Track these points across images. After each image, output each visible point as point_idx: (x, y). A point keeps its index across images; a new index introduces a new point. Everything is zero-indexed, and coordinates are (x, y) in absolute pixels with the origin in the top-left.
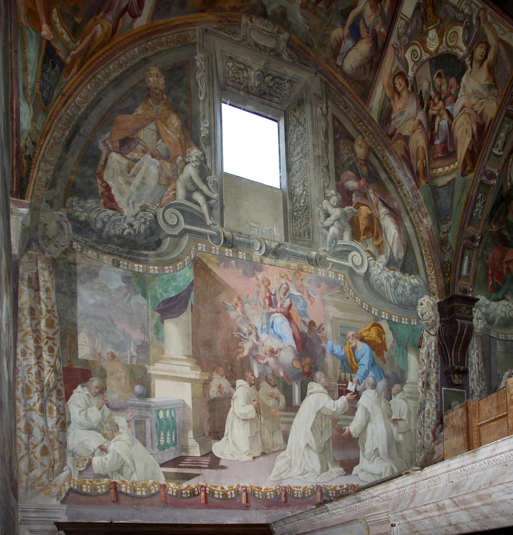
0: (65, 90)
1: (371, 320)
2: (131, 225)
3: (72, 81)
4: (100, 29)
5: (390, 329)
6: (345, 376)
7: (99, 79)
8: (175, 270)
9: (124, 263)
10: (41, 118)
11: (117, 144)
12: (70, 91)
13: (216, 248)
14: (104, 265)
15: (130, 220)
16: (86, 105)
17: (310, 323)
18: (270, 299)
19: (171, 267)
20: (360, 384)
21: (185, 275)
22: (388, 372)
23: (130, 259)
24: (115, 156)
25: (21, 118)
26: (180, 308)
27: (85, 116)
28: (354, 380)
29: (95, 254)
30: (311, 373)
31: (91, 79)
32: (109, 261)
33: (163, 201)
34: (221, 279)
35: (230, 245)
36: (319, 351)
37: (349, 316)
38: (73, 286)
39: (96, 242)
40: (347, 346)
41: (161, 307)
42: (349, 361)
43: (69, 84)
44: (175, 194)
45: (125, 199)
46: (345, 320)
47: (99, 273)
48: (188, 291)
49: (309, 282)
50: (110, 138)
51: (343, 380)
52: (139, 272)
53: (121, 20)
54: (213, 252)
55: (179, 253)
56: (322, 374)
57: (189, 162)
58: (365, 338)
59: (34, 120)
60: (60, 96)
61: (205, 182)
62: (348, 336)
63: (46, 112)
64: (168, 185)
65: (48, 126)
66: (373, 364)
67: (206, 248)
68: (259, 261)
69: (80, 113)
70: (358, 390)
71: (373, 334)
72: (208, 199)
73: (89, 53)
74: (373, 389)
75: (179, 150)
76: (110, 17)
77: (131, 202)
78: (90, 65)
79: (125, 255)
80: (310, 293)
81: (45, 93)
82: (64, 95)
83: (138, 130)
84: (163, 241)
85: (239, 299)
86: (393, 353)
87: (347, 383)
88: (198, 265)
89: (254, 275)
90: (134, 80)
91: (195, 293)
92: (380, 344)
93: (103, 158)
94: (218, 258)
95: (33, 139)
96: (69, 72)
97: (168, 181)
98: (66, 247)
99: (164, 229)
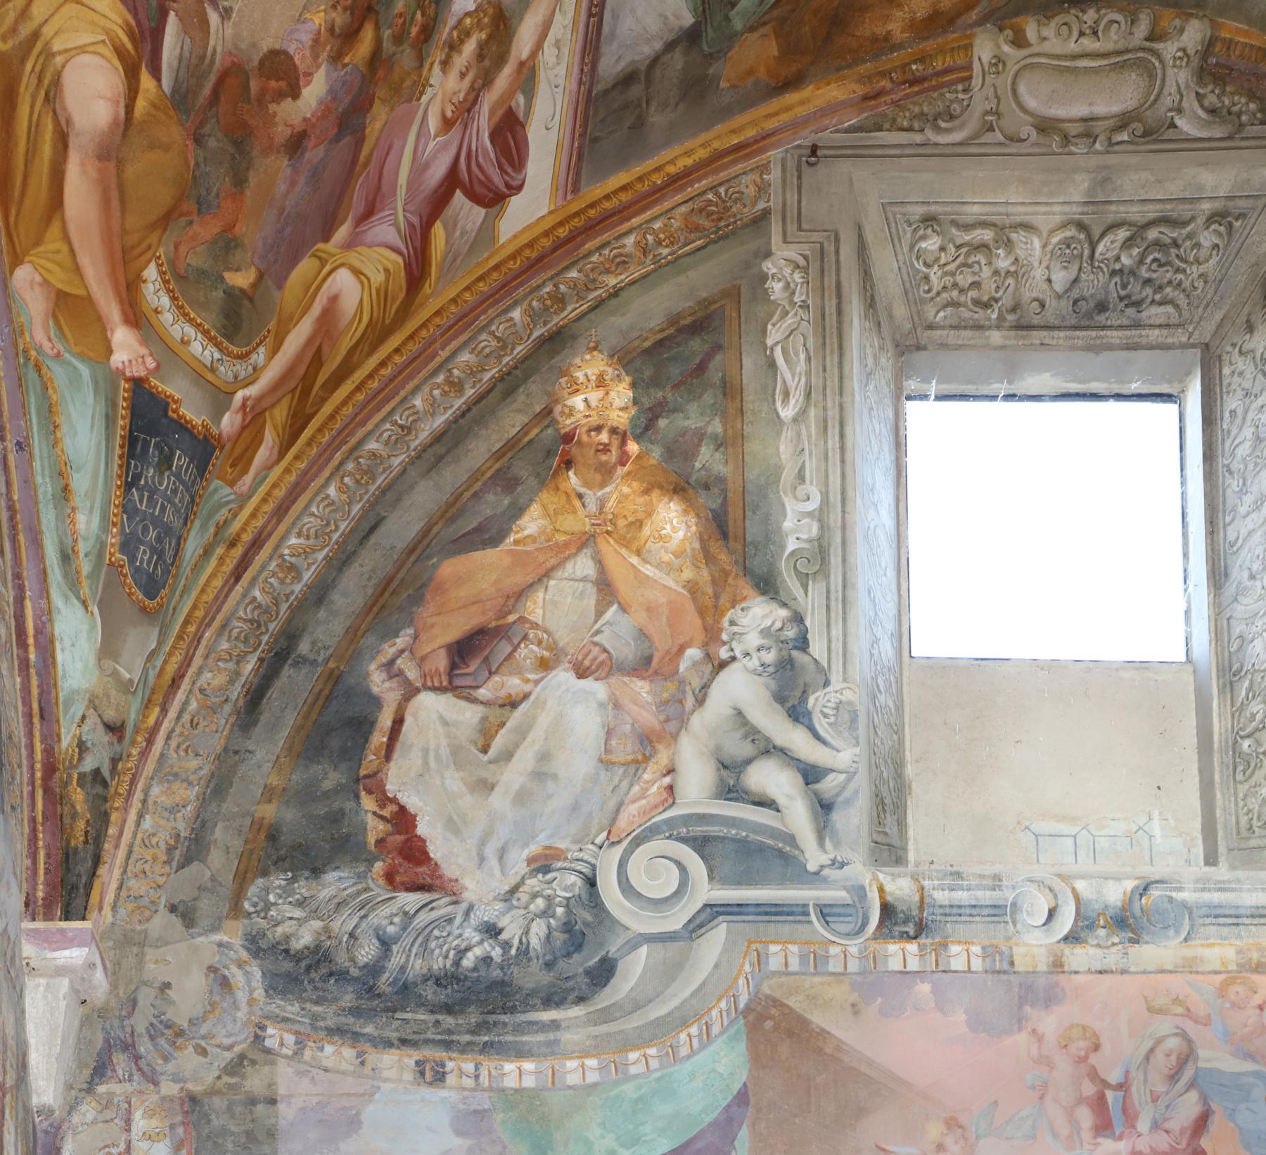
2: (492, 931)
4: (351, 278)
8: (672, 1056)
9: (460, 1067)
10: (140, 641)
13: (847, 952)
14: (386, 1087)
18: (1099, 1105)
19: (652, 1051)
23: (486, 1048)
24: (430, 705)
25: (59, 657)
29: (348, 1053)
32: (402, 1068)
33: (623, 822)
35: (911, 929)
39: (356, 1012)
44: (670, 788)
47: (363, 1117)
53: (438, 230)
59: (108, 649)
64: (640, 762)
65: (177, 659)
67: (803, 958)
68: (1042, 967)
72: (810, 774)
73: (321, 379)
76: (387, 230)
78: (332, 417)
79: (467, 1038)
84: (621, 966)
85: (952, 1124)
88: (769, 1024)
89: (1021, 1021)
95: (111, 715)
96: (242, 461)
98: (237, 1049)
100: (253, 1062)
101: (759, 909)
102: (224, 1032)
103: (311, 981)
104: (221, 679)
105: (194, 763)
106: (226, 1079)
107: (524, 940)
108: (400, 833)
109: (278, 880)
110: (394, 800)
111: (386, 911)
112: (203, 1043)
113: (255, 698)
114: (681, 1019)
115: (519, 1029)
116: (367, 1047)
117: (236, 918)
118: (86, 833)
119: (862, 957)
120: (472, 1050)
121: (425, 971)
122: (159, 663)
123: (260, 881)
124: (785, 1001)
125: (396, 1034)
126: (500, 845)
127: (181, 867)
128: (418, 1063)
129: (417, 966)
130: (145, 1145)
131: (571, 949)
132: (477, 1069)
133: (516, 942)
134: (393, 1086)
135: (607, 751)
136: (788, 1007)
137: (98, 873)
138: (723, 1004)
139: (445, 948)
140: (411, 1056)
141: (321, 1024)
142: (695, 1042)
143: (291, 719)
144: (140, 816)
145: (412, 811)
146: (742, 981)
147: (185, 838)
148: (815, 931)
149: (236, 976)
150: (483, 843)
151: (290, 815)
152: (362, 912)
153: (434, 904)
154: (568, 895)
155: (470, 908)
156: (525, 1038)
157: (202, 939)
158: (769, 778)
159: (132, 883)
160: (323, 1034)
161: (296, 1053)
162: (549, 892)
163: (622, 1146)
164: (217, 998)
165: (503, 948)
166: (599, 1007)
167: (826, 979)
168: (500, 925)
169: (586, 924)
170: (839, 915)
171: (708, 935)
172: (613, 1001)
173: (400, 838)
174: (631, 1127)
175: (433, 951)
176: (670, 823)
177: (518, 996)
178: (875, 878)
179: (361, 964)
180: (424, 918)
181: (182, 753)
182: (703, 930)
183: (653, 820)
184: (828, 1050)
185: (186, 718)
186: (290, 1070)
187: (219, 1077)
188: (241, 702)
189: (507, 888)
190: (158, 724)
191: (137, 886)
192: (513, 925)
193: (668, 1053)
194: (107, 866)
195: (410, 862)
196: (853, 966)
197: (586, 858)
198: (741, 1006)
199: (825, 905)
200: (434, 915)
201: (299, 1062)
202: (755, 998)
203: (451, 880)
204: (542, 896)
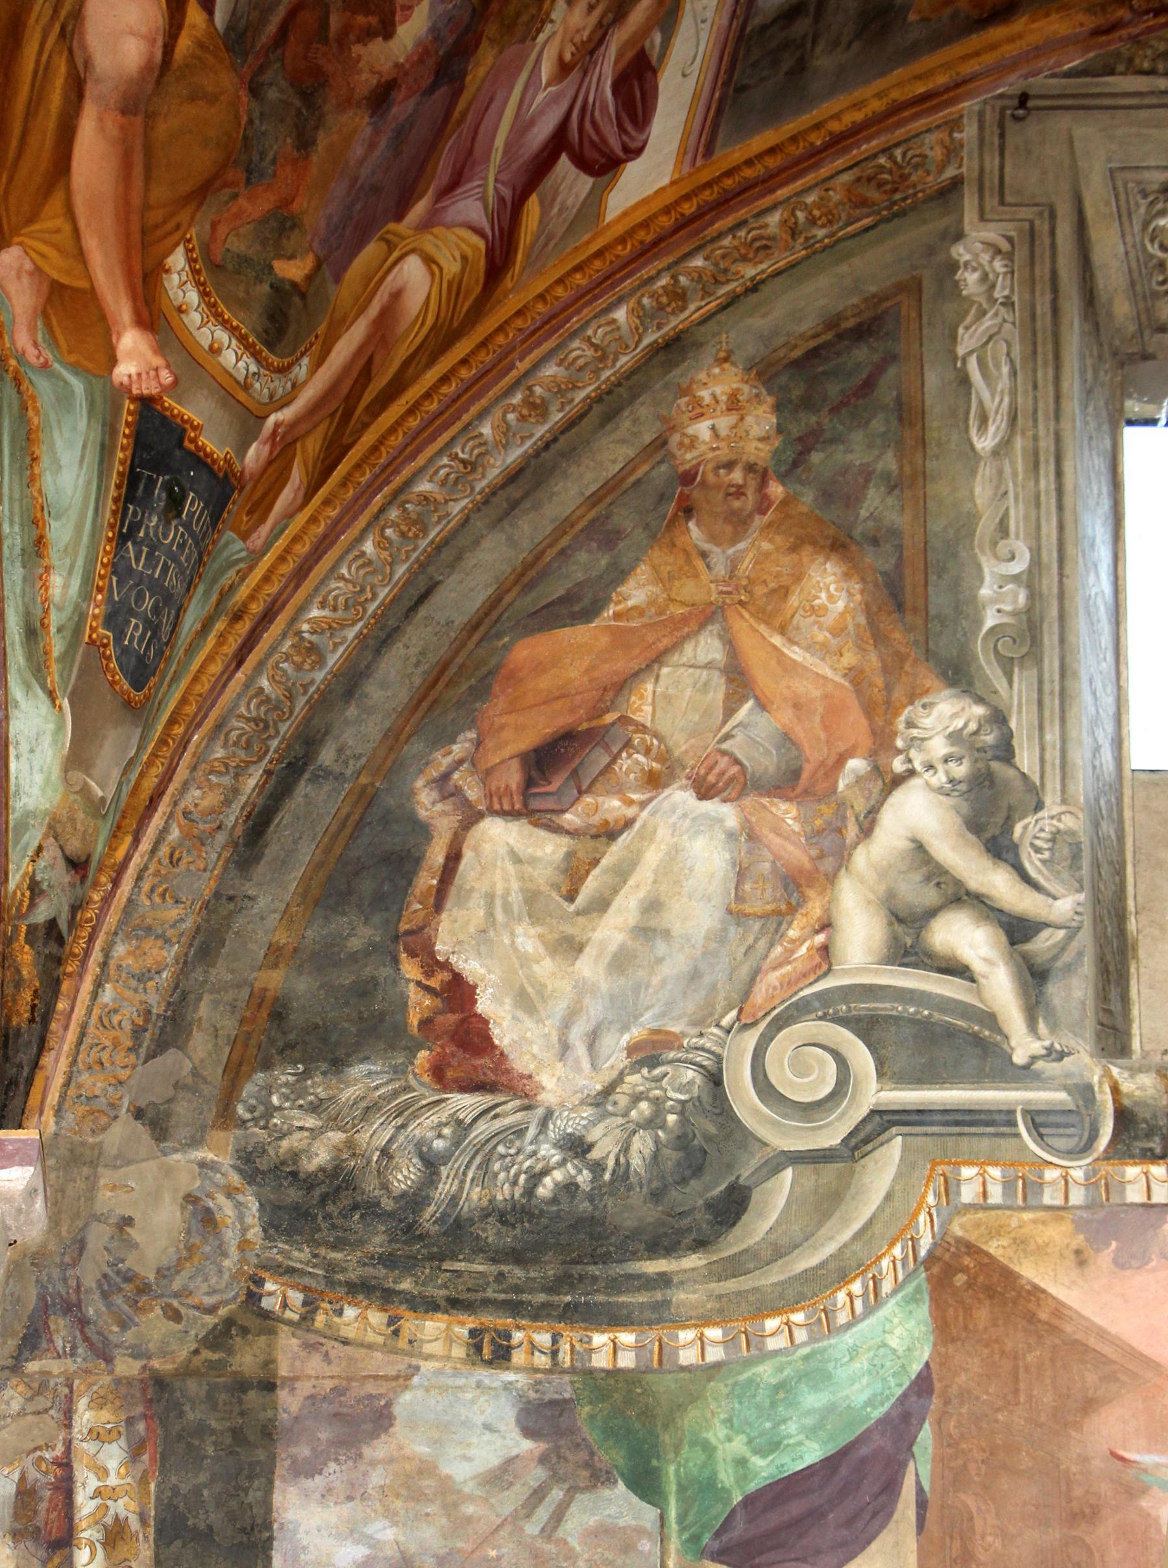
0: (243, 592)
2: (577, 1147)
3: (281, 543)
7: (425, 499)
9: (532, 1340)
11: (513, 777)
12: (272, 589)
13: (1066, 1178)
14: (427, 1366)
15: (566, 1124)
16: (351, 633)
19: (798, 1317)
21: (881, 1344)
26: (849, 1522)
27: (350, 682)
29: (377, 1318)
31: (382, 510)
32: (450, 1340)
33: (759, 996)
34: (1102, 1334)
38: (254, 1496)
39: (388, 1260)
41: (740, 1529)
43: (268, 559)
44: (825, 950)
45: (551, 1027)
47: (397, 1410)
48: (901, 1423)
50: (472, 759)
52: (614, 1373)
54: (1050, 1197)
55: (847, 1235)
57: (912, 773)
60: (220, 625)
61: (1001, 849)
63: (136, 711)
67: (1008, 1185)
69: (319, 676)
72: (1017, 930)
75: (855, 725)
77: (577, 1035)
79: (541, 1297)
81: (134, 629)
82: (237, 617)
83: (622, 685)
84: (756, 1196)
88: (960, 1279)
90: (611, 454)
91: (940, 1435)
93: (437, 855)
94: (1080, 1226)
97: (786, 893)
98: (223, 1312)
99: (762, 1131)
100: (245, 1331)
101: (948, 1118)
102: (204, 1287)
103: (328, 1216)
104: (211, 799)
105: (174, 913)
106: (206, 1354)
107: (622, 1160)
108: (452, 1011)
109: (285, 1076)
110: (446, 966)
111: (431, 1119)
112: (175, 1303)
113: (259, 824)
114: (838, 1272)
115: (616, 1285)
116: (402, 1310)
117: (225, 1127)
118: (33, 1007)
119: (1090, 1183)
120: (549, 1315)
121: (485, 1202)
122: (134, 776)
123: (260, 1077)
124: (984, 1247)
125: (443, 1292)
126: (590, 1027)
127: (151, 1056)
128: (473, 1333)
129: (475, 1195)
130: (90, 1447)
131: (687, 1173)
132: (555, 1341)
133: (611, 1163)
134: (437, 1364)
135: (739, 898)
136: (988, 1254)
137: (41, 1063)
138: (897, 1251)
139: (513, 1171)
140: (463, 1324)
141: (340, 1277)
142: (858, 1304)
143: (306, 853)
144: (98, 985)
145: (471, 980)
146: (923, 1218)
147: (159, 1016)
148: (1025, 1147)
149: (225, 1208)
150: (566, 1024)
151: (303, 985)
152: (400, 1121)
153: (498, 1110)
154: (683, 1097)
155: (548, 1115)
156: (623, 1299)
157: (177, 1156)
158: (963, 936)
159: (85, 1078)
160: (342, 1291)
161: (303, 1318)
162: (658, 1092)
163: (756, 1452)
164: (195, 1239)
165: (592, 1171)
166: (725, 1254)
167: (1040, 1214)
168: (590, 1138)
169: (708, 1138)
170: (1058, 1125)
171: (876, 1154)
172: (744, 1246)
173: (452, 1018)
174: (768, 1425)
175: (496, 1175)
176: (825, 998)
177: (613, 1239)
178: (1107, 1074)
179: (396, 1193)
180: (483, 1129)
181: (157, 900)
182: (869, 1147)
183: (802, 994)
184: (1043, 1316)
185: (164, 850)
186: (295, 1341)
187: (196, 1352)
188: (239, 831)
189: (599, 1087)
190: (128, 858)
191: (92, 1083)
192: (607, 1140)
193: (820, 1319)
194: (53, 1053)
195: (465, 1049)
196: (1077, 1197)
197: (708, 1045)
198: (923, 1253)
199: (1040, 1112)
200: (498, 1124)
201: (308, 1330)
202: (942, 1242)
203: (522, 1076)
204: (647, 1099)
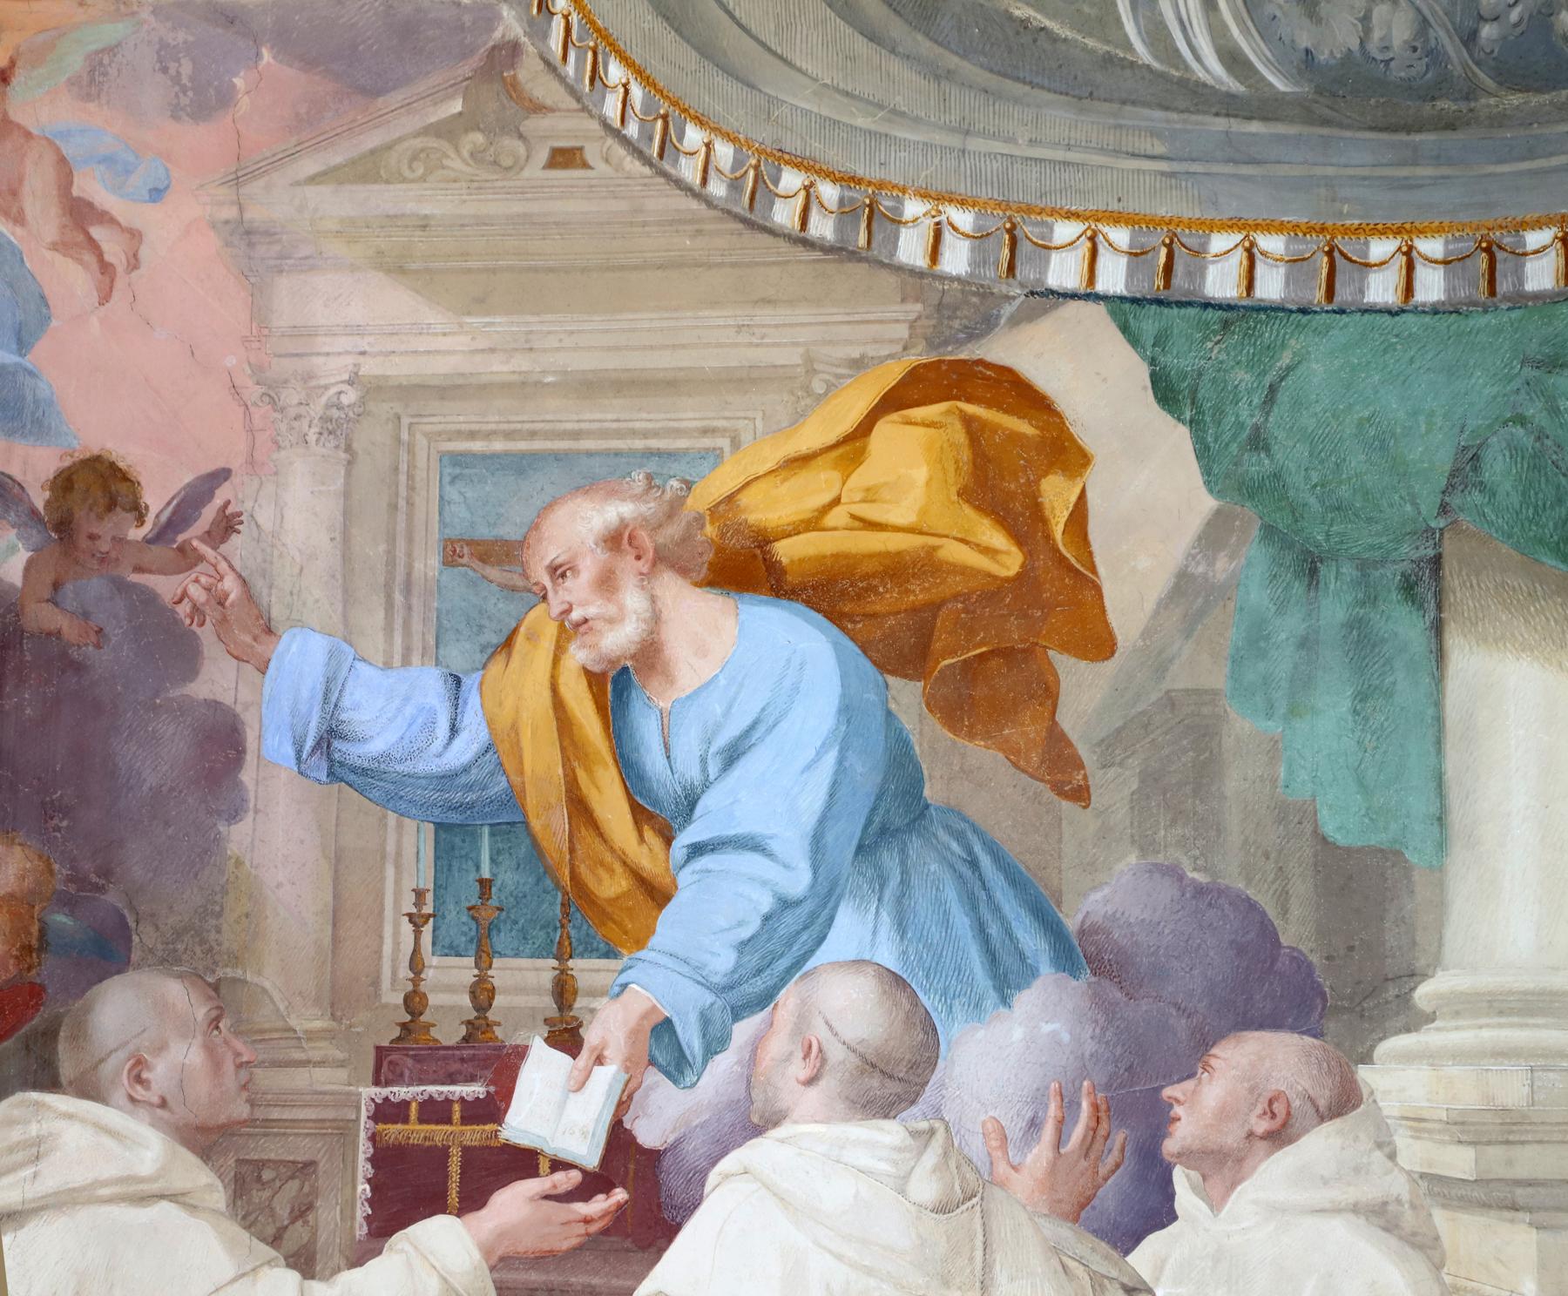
1: (889, 337)
5: (1166, 391)
6: (482, 994)
17: (64, 483)
20: (678, 1066)
22: (1111, 889)
28: (609, 1025)
30: (36, 993)
36: (155, 758)
37: (576, 341)
40: (532, 661)
42: (551, 824)
46: (525, 388)
49: (93, 81)
51: (449, 1033)
56: (175, 991)
58: (785, 551)
62: (550, 550)
66: (889, 818)
70: (649, 1134)
71: (908, 483)
74: (885, 1108)
80: (92, 187)
86: (1201, 668)
87: (503, 1068)
92: (993, 591)
